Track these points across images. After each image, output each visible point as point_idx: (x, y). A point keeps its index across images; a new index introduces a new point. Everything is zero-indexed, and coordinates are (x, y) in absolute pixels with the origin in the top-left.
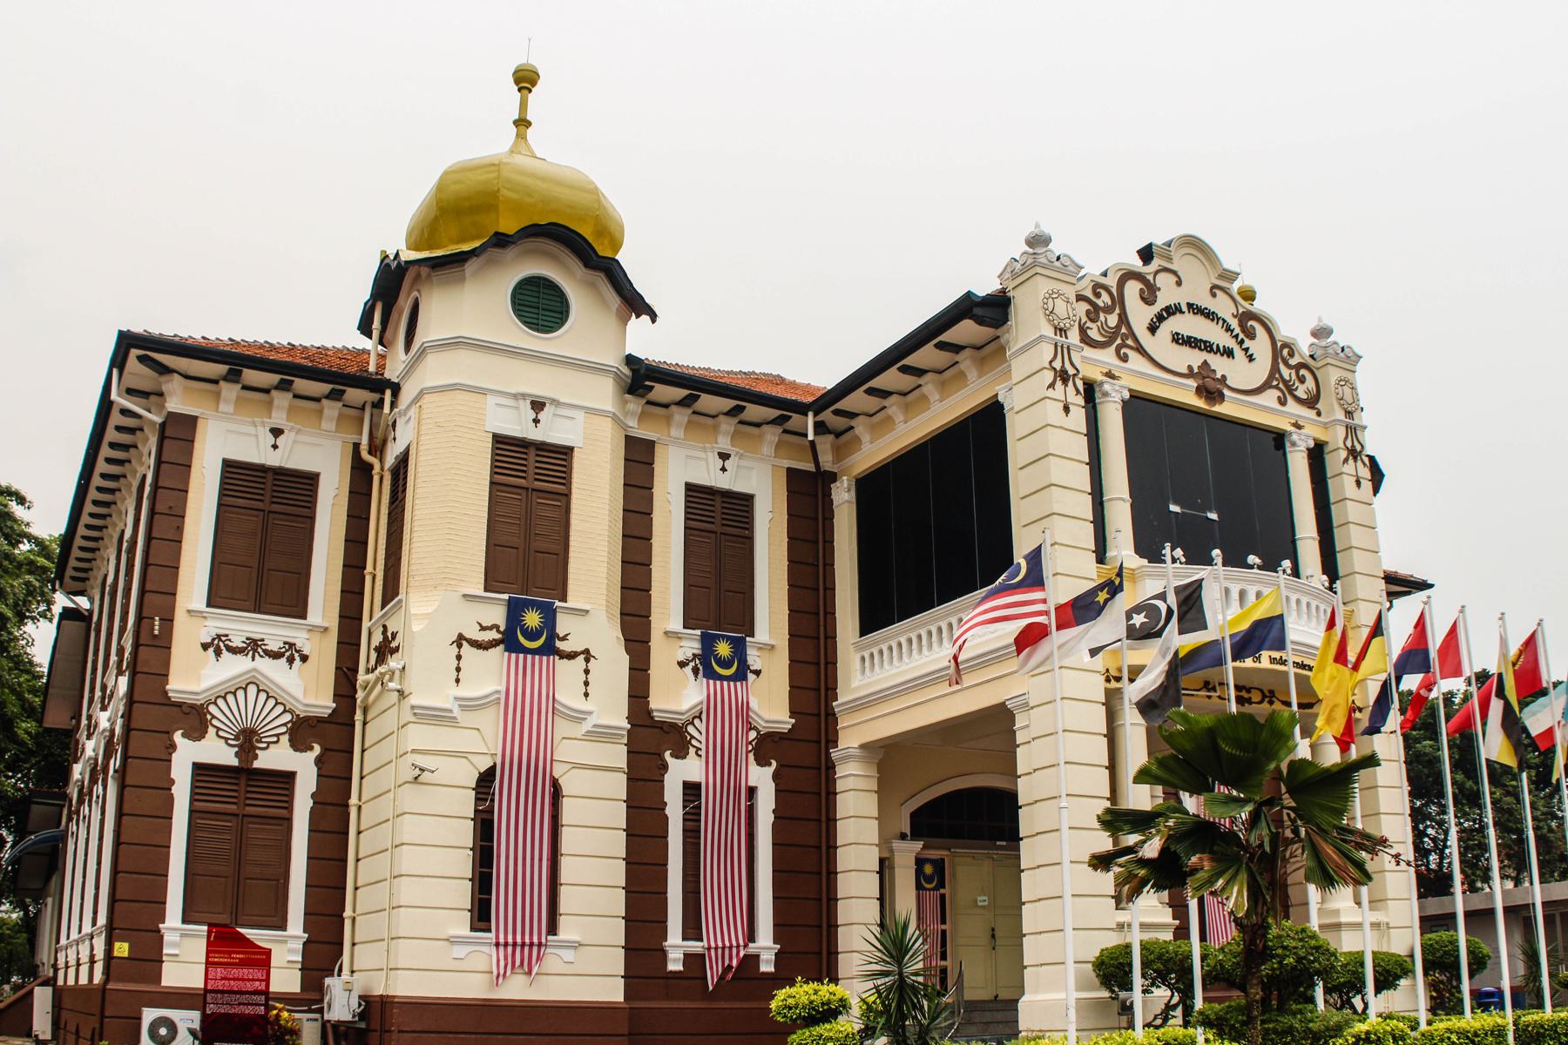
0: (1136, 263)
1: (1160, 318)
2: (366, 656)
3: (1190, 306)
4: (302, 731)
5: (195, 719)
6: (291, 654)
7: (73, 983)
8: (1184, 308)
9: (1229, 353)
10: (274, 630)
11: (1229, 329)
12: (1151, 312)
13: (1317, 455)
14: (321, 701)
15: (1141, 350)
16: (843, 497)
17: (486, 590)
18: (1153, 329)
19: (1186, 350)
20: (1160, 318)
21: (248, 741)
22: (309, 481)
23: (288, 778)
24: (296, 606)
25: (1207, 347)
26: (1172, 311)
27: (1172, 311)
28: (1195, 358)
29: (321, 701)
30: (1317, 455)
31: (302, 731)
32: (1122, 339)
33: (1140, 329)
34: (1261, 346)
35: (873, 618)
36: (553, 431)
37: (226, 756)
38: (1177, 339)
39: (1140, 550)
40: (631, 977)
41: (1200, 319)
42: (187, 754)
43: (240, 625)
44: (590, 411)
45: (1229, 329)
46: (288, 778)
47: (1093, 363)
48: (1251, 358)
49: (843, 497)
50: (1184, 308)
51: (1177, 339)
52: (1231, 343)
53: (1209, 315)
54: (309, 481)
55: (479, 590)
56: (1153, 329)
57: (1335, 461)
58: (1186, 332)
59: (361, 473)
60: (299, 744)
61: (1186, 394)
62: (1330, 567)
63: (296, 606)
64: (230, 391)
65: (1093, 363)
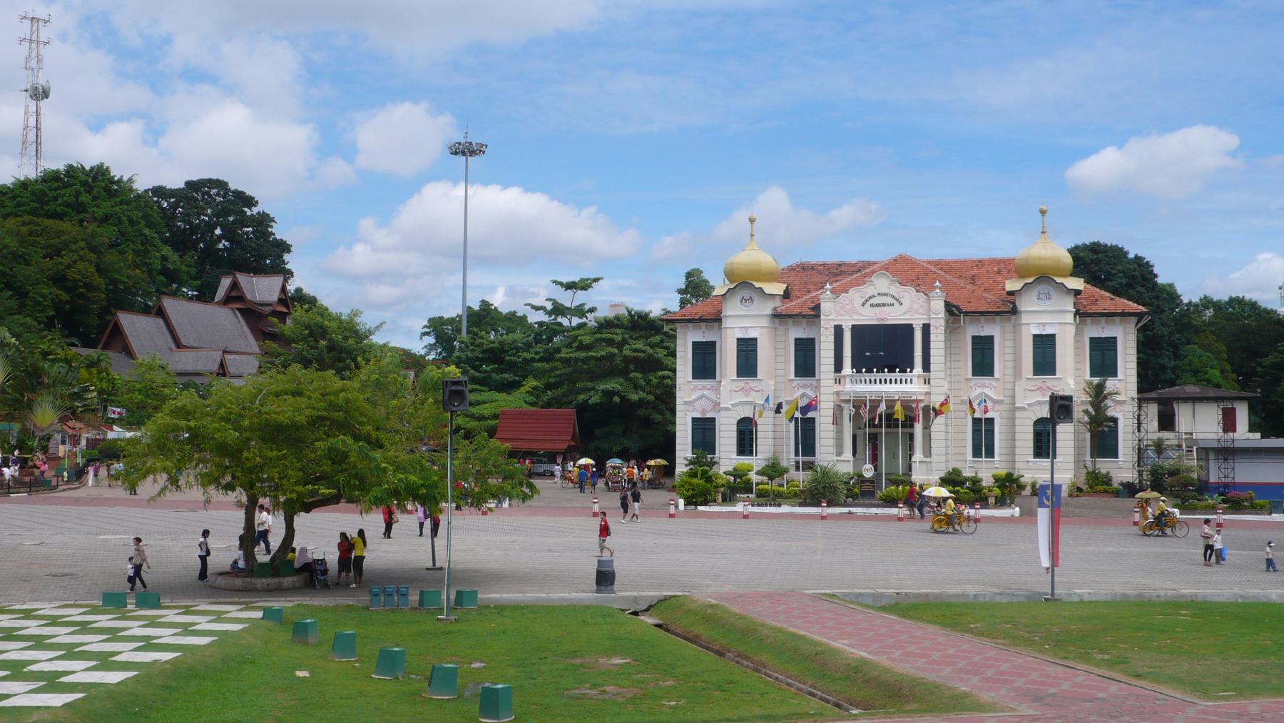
1: (867, 301)
3: (879, 294)
8: (876, 295)
9: (892, 305)
11: (893, 297)
12: (864, 300)
15: (858, 314)
17: (738, 377)
18: (863, 305)
19: (875, 308)
20: (867, 301)
25: (884, 305)
26: (870, 298)
27: (870, 298)
36: (751, 335)
38: (872, 305)
41: (882, 297)
44: (761, 327)
45: (893, 297)
48: (901, 304)
50: (876, 295)
51: (872, 305)
52: (893, 301)
53: (885, 295)
55: (736, 378)
56: (863, 305)
58: (875, 303)
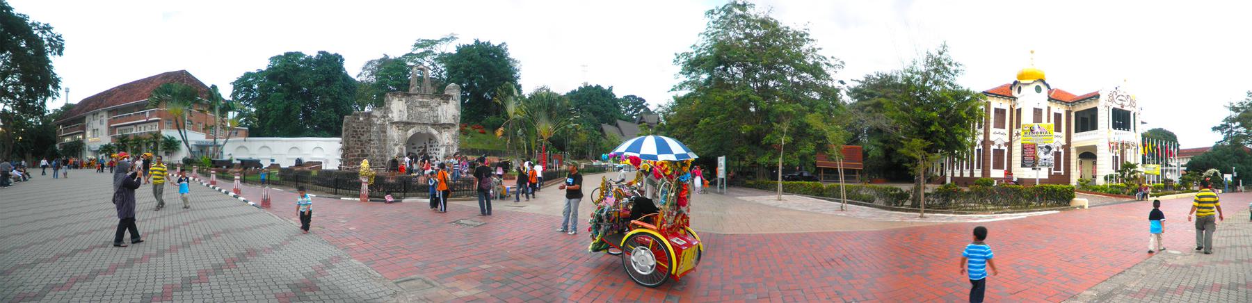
0: (1115, 90)
2: (1014, 134)
4: (1006, 144)
5: (993, 143)
6: (1004, 134)
7: (968, 176)
10: (1002, 131)
13: (1134, 114)
14: (1008, 141)
16: (1073, 115)
21: (999, 146)
22: (1005, 110)
23: (1003, 150)
24: (1004, 128)
28: (1121, 102)
29: (1008, 141)
30: (1134, 114)
31: (1006, 144)
32: (1113, 101)
33: (1115, 98)
34: (1129, 100)
35: (1076, 132)
37: (997, 148)
39: (1113, 127)
40: (1049, 176)
42: (992, 148)
43: (998, 130)
46: (1003, 150)
47: (1109, 104)
49: (1073, 115)
54: (1005, 110)
57: (1136, 115)
59: (1012, 109)
60: (1005, 146)
61: (1119, 107)
62: (1134, 129)
63: (1004, 128)
64: (995, 98)
65: (1109, 104)
